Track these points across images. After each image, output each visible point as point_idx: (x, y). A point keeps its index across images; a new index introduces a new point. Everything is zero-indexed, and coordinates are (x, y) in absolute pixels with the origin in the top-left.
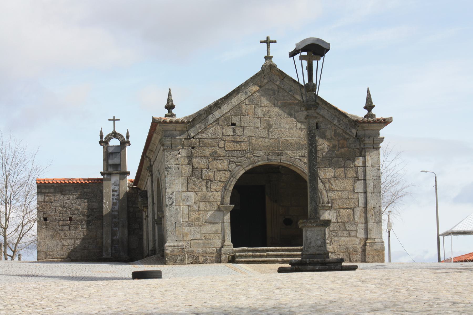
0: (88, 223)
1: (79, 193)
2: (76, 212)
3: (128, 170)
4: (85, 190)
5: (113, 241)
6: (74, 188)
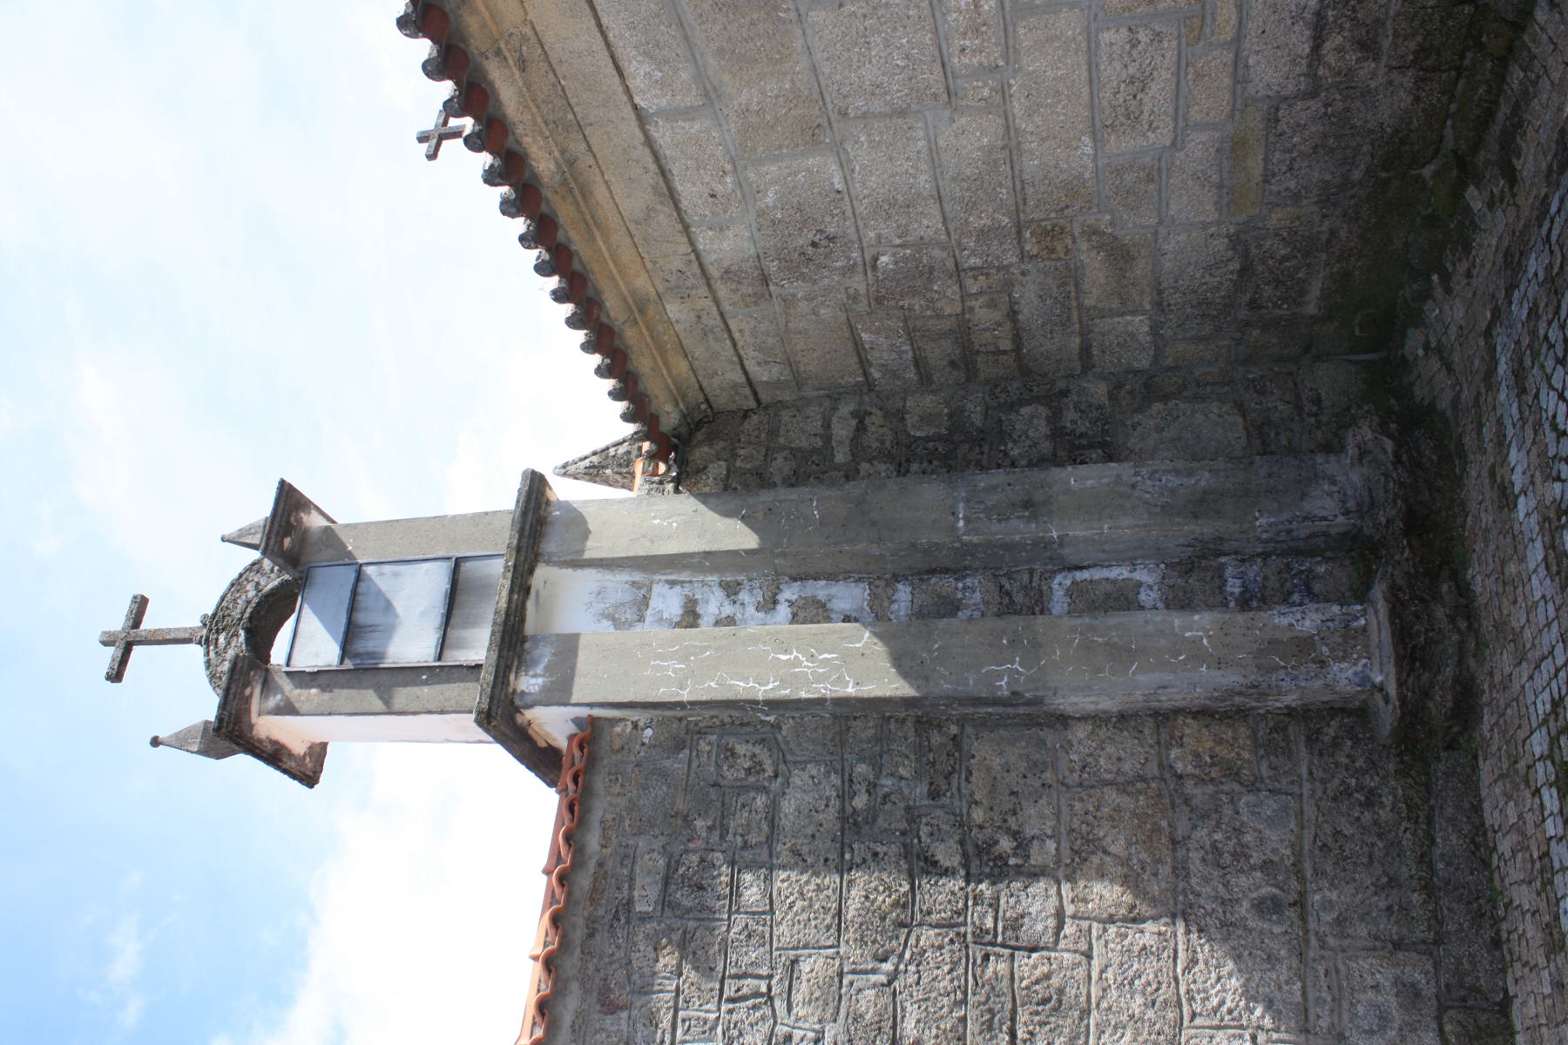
0: (990, 863)
1: (667, 960)
2: (868, 1002)
3: (506, 498)
4: (645, 897)
5: (1179, 602)
6: (611, 1008)
